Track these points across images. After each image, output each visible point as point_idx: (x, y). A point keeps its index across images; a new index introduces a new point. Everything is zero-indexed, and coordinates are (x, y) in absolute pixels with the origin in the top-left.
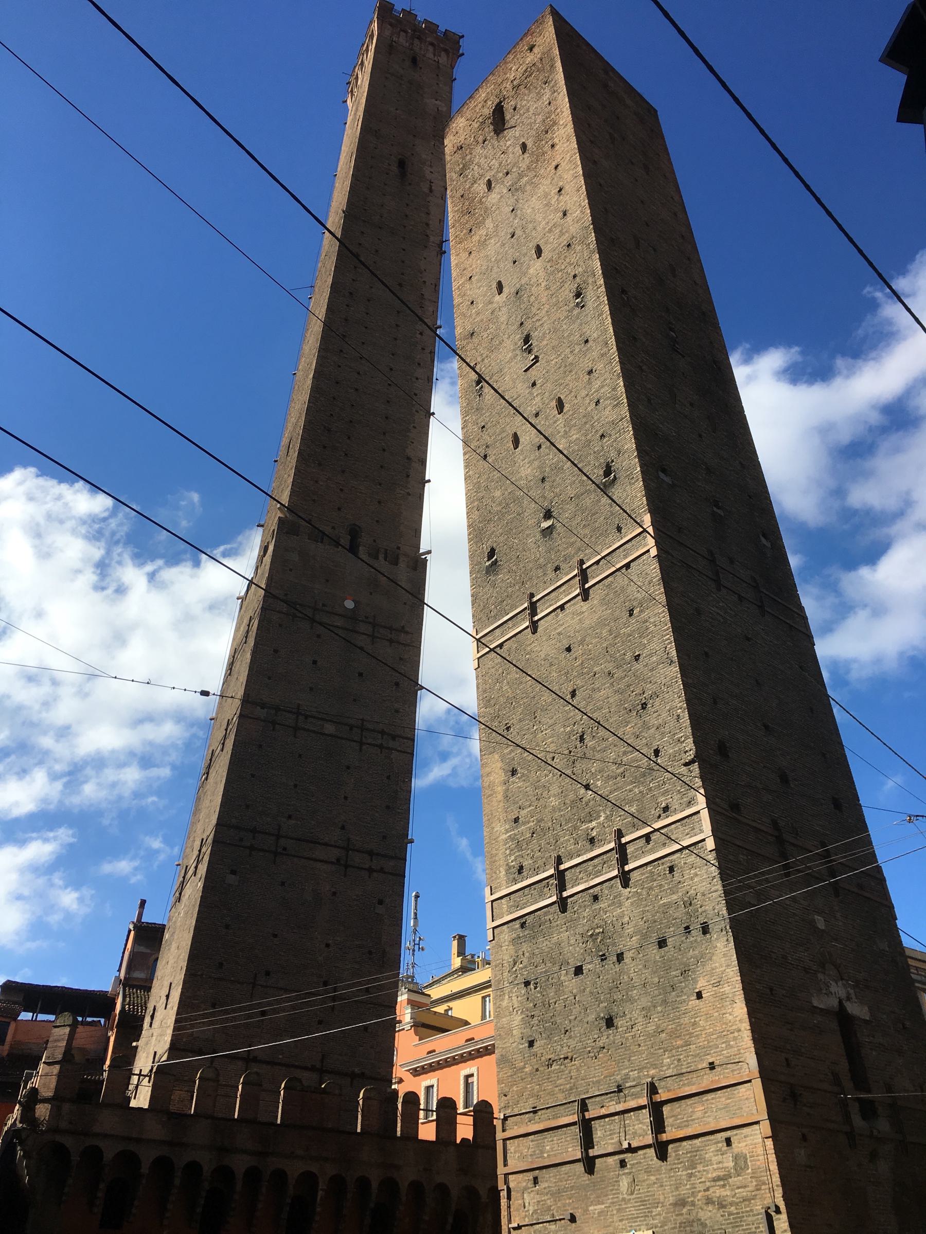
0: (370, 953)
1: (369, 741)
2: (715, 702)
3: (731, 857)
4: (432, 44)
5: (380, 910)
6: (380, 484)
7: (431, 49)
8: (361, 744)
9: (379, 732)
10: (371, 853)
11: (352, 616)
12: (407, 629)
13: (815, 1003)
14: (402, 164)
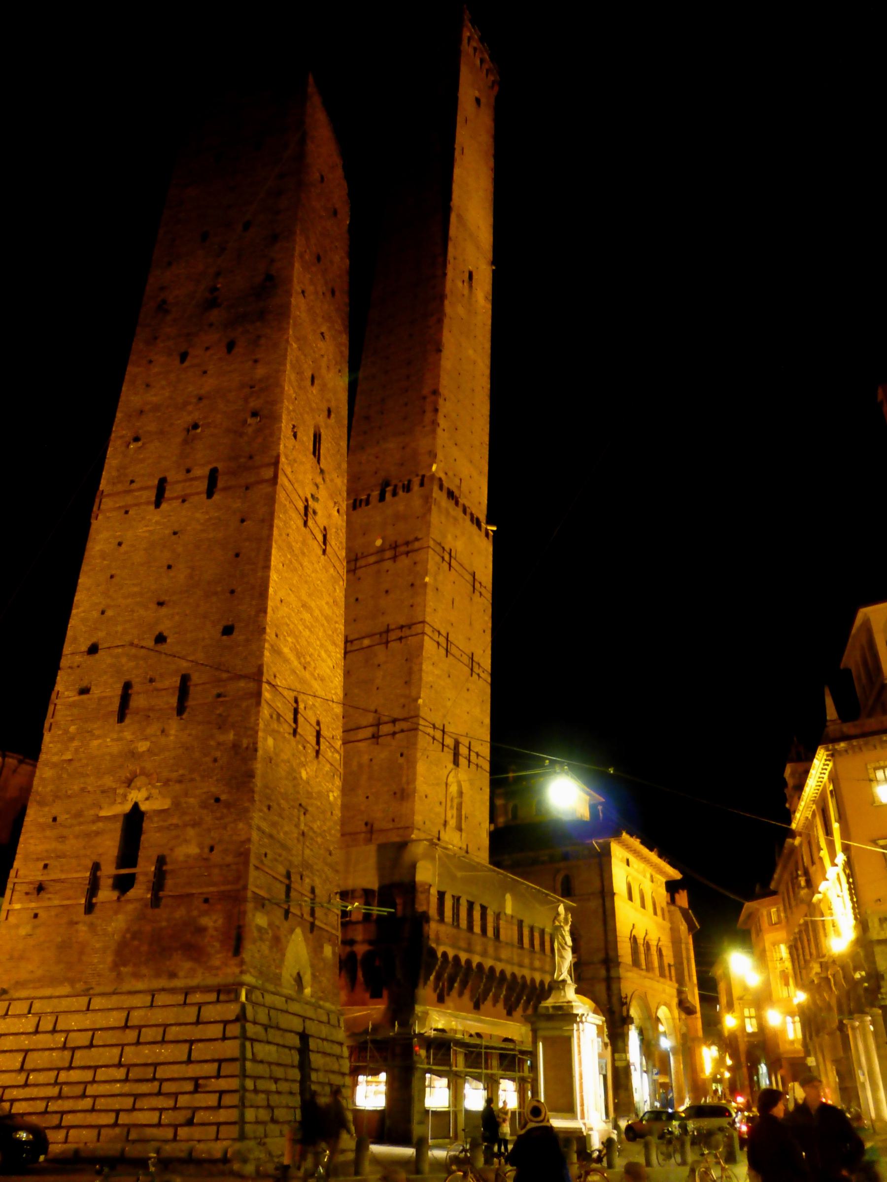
1: (394, 638)
2: (103, 613)
5: (401, 760)
8: (387, 643)
10: (394, 721)
11: (381, 550)
12: (420, 536)
13: (103, 813)
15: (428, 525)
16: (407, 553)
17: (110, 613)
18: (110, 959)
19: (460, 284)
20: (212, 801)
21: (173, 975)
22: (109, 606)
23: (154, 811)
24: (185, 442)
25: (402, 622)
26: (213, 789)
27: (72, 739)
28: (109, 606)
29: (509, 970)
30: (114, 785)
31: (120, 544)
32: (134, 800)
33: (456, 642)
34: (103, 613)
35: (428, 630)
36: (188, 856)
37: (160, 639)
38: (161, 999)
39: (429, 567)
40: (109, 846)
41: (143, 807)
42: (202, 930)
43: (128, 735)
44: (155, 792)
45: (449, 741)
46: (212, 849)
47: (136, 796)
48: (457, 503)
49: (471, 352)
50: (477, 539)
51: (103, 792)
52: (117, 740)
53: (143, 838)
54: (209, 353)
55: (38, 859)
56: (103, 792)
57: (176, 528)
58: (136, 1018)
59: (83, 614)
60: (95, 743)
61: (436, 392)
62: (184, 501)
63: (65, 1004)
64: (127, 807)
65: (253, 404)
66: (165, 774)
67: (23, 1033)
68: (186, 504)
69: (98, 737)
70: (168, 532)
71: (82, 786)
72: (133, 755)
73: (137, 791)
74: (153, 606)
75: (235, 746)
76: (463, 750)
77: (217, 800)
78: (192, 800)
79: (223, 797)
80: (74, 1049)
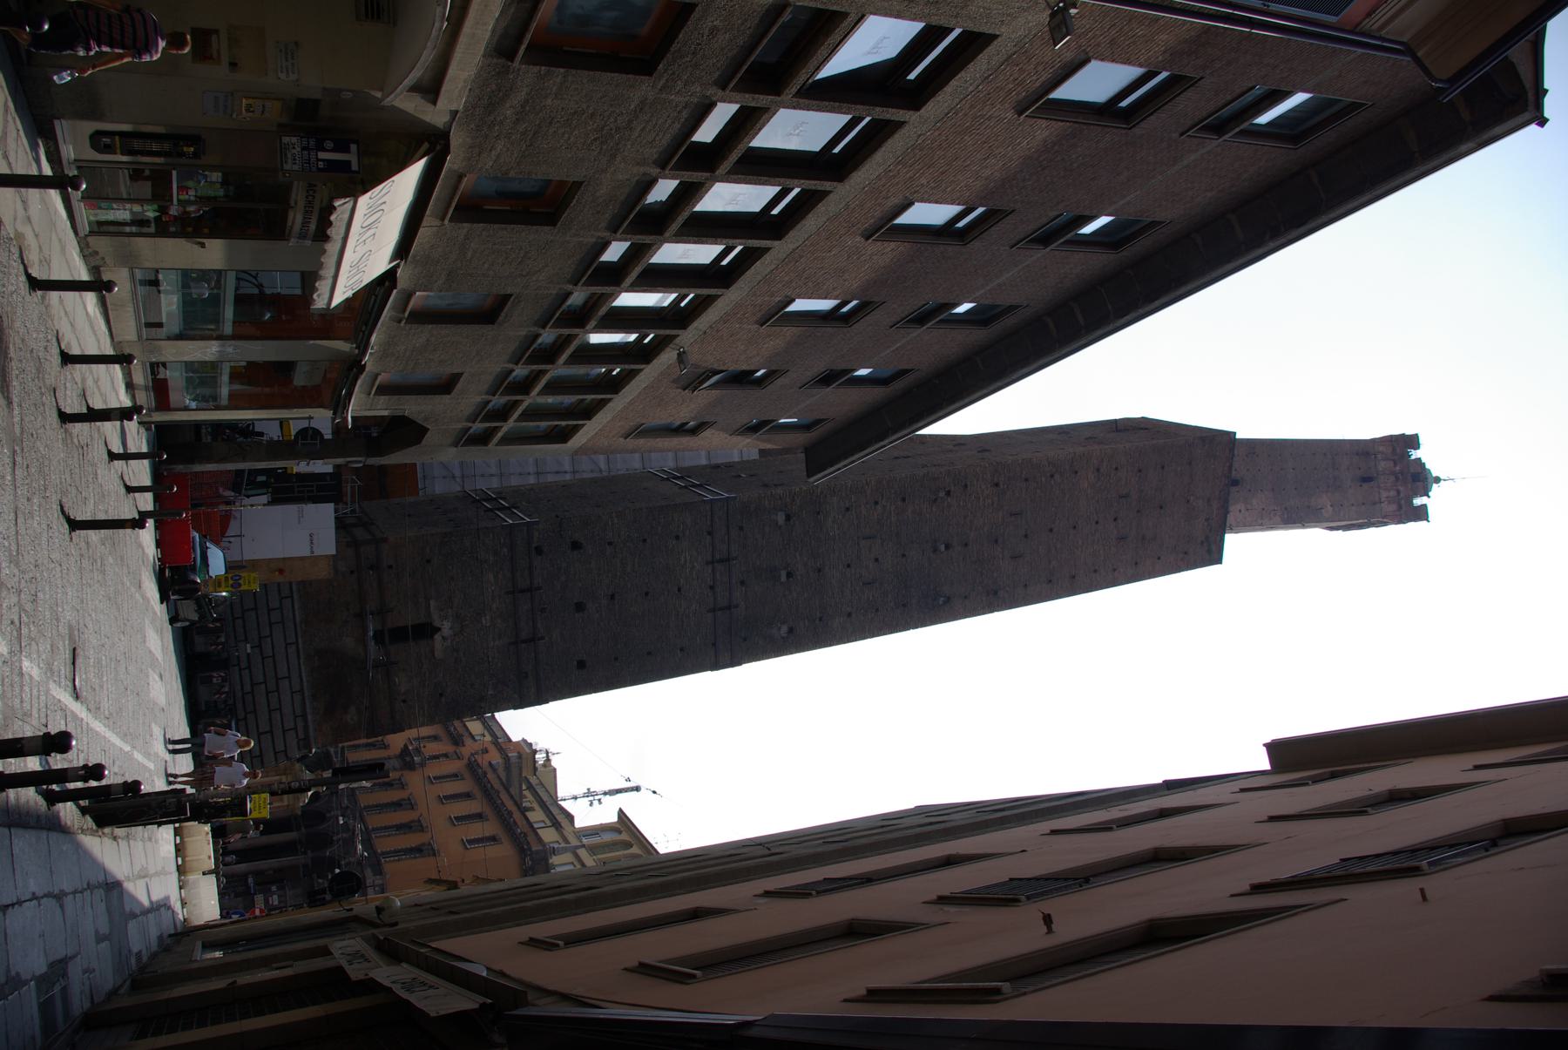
4: (1398, 492)
7: (1392, 493)
13: (432, 603)
31: (677, 537)
37: (580, 607)
38: (297, 698)
58: (285, 684)
60: (491, 577)
64: (437, 623)
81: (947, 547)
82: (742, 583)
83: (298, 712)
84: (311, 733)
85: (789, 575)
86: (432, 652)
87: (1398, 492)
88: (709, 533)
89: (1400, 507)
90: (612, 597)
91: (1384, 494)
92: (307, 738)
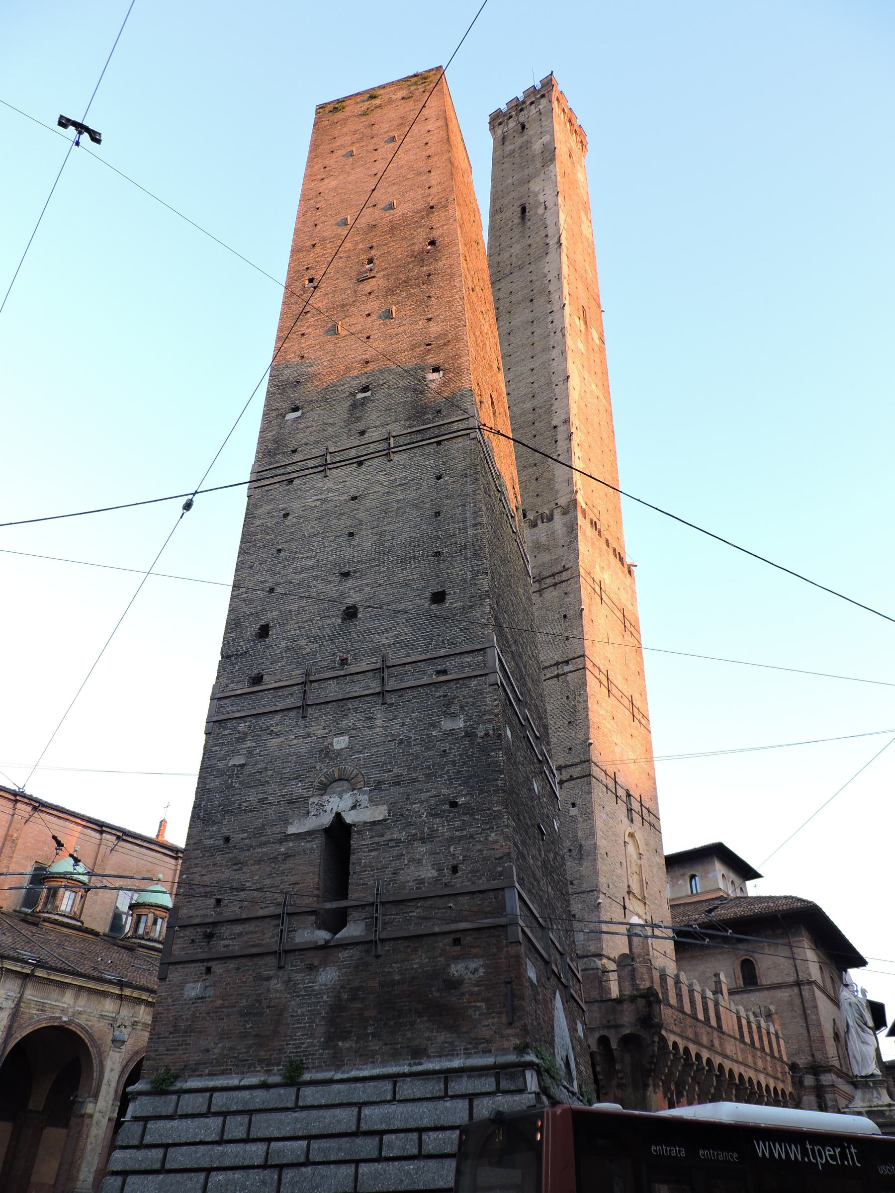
0: (570, 850)
3: (227, 732)
4: (532, 103)
5: (573, 811)
6: (535, 465)
7: (533, 106)
9: (555, 665)
12: (567, 567)
13: (291, 830)
14: (524, 210)
15: (576, 551)
16: (555, 585)
17: (279, 590)
18: (320, 1031)
19: (577, 320)
20: (447, 807)
21: (418, 1053)
22: (278, 584)
23: (365, 823)
24: (354, 406)
25: (557, 658)
26: (445, 791)
27: (243, 738)
28: (278, 584)
29: (737, 1069)
30: (305, 793)
31: (286, 515)
32: (334, 811)
33: (615, 682)
34: (272, 590)
35: (589, 665)
36: (421, 882)
37: (351, 613)
38: (407, 1089)
39: (583, 597)
40: (307, 872)
41: (348, 820)
42: (454, 984)
43: (318, 730)
44: (364, 799)
45: (621, 793)
46: (455, 870)
47: (338, 803)
48: (600, 535)
49: (594, 387)
50: (621, 575)
51: (290, 802)
52: (304, 737)
53: (353, 858)
54: (370, 319)
55: (206, 895)
56: (290, 802)
57: (353, 492)
58: (373, 1117)
59: (245, 596)
60: (275, 741)
61: (567, 421)
62: (360, 464)
63: (260, 1098)
64: (326, 820)
65: (432, 360)
66: (376, 776)
67: (201, 1143)
68: (364, 468)
69: (278, 735)
70: (346, 497)
71: (261, 796)
72: (327, 753)
73: (337, 799)
74: (336, 579)
75: (470, 734)
76: (636, 806)
77: (454, 804)
78: (416, 807)
79: (461, 800)
80: (281, 1167)
81: (370, 261)
82: (362, 433)
83: (437, 1087)
84: (490, 1060)
85: (365, 389)
86: (374, 823)
87: (532, 103)
88: (291, 481)
89: (543, 96)
90: (346, 575)
91: (534, 111)
92: (497, 1070)
